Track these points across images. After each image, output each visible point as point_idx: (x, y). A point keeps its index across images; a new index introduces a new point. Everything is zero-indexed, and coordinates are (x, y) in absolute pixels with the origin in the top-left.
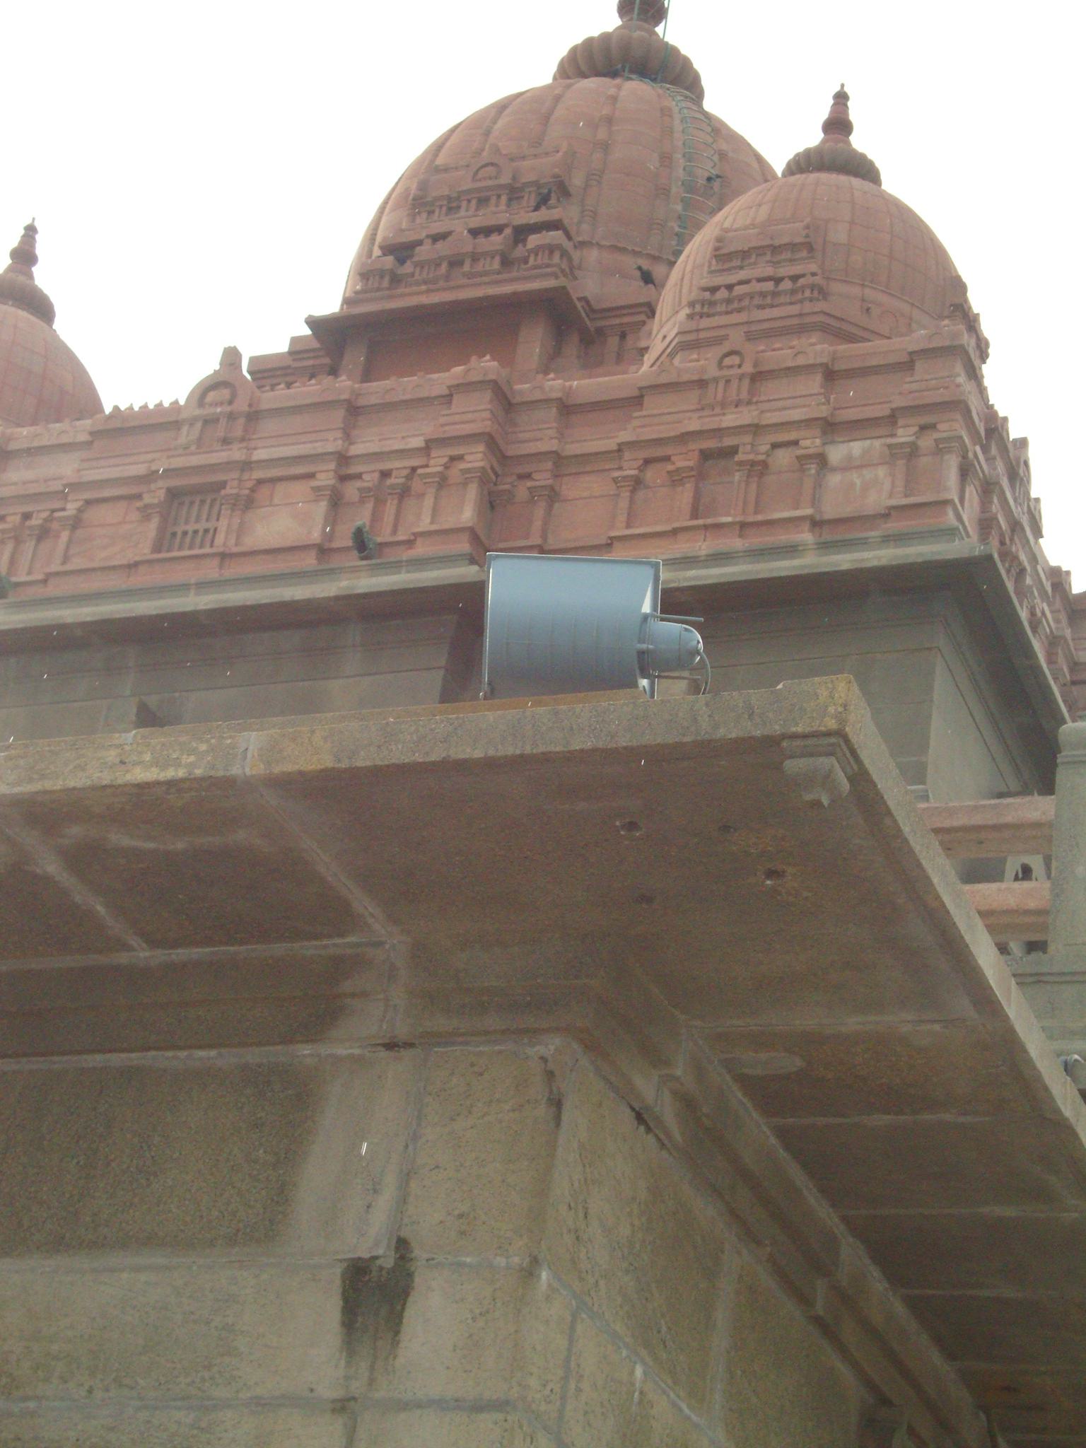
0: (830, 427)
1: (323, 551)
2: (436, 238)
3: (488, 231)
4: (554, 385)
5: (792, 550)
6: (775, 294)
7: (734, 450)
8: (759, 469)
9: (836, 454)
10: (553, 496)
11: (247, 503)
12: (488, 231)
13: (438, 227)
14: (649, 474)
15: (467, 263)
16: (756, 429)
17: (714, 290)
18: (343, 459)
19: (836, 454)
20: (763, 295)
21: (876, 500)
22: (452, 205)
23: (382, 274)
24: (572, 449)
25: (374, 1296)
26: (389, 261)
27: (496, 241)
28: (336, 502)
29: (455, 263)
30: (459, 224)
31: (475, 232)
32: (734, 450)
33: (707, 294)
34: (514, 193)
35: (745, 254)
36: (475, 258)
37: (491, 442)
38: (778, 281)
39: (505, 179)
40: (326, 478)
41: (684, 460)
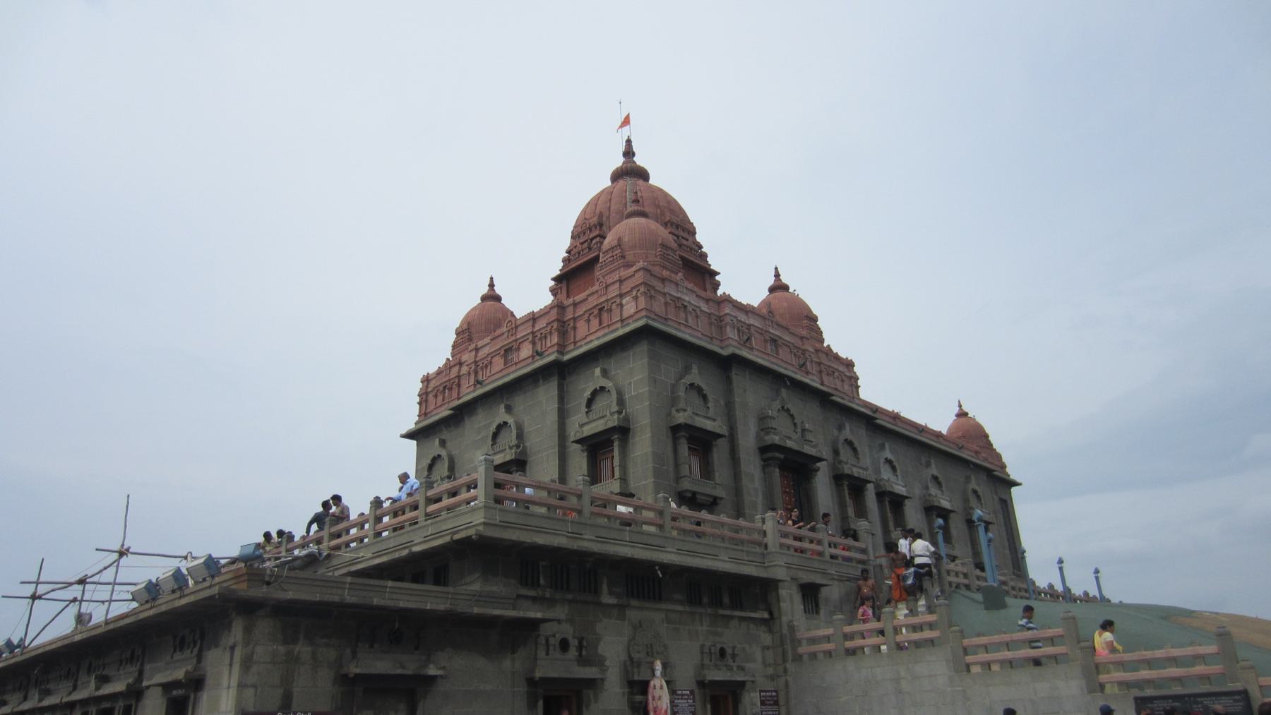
0: (621, 296)
1: (533, 357)
4: (571, 300)
5: (616, 330)
8: (610, 310)
9: (624, 302)
10: (575, 328)
11: (518, 349)
18: (533, 333)
19: (624, 302)
21: (633, 311)
25: (233, 648)
28: (534, 343)
37: (558, 320)
40: (530, 337)
41: (596, 312)
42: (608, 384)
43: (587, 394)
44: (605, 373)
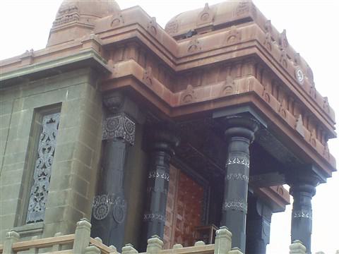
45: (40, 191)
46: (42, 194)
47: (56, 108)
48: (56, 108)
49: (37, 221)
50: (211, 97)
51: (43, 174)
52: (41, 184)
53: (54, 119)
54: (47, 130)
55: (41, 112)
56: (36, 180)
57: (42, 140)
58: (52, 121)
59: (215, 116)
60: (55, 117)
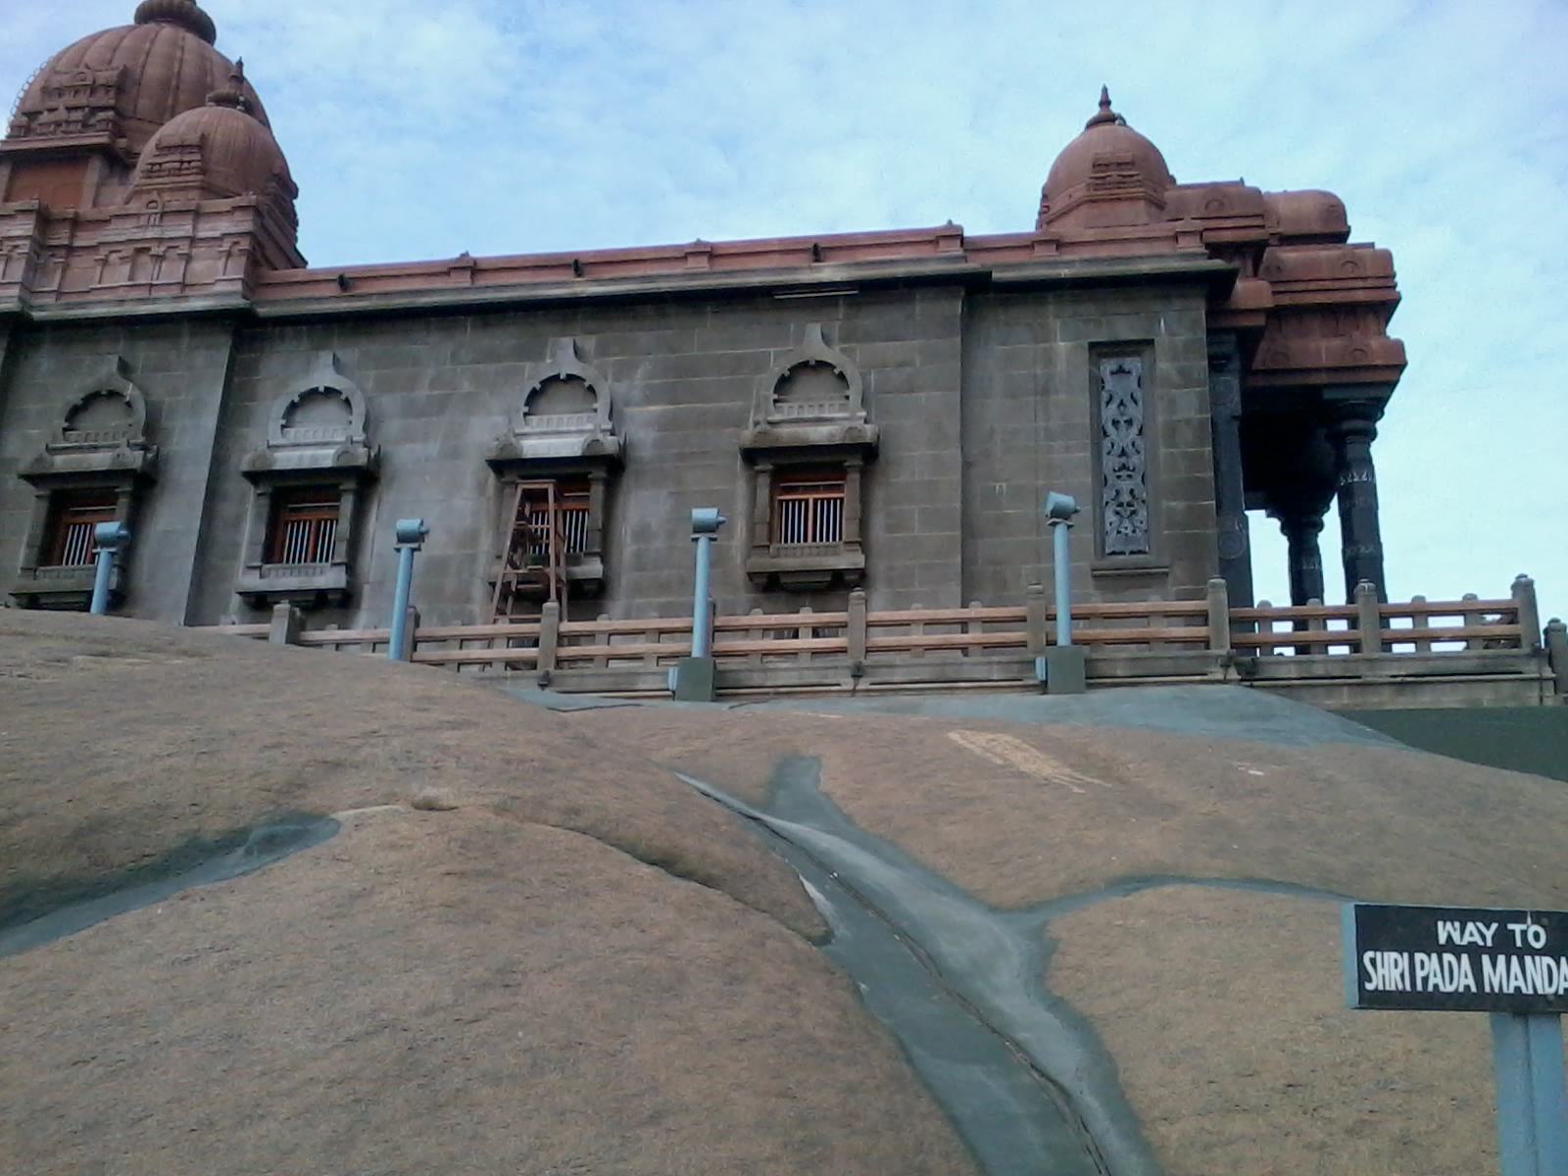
2: (52, 110)
3: (76, 108)
6: (180, 169)
7: (149, 249)
12: (76, 108)
13: (51, 104)
14: (113, 257)
15: (64, 125)
16: (160, 240)
17: (153, 165)
20: (174, 169)
22: (60, 92)
23: (20, 127)
24: (78, 243)
26: (25, 119)
27: (78, 115)
29: (58, 124)
30: (59, 104)
31: (69, 109)
32: (149, 249)
33: (150, 167)
34: (93, 89)
35: (169, 148)
36: (68, 122)
38: (182, 162)
39: (89, 82)
41: (128, 251)
42: (130, 391)
43: (75, 397)
44: (125, 368)
45: (1126, 498)
46: (1129, 505)
47: (1141, 346)
48: (1141, 346)
49: (1132, 553)
50: (1324, 362)
51: (1124, 467)
52: (1125, 485)
53: (1126, 367)
54: (1110, 384)
55: (1099, 350)
56: (1111, 479)
57: (1108, 403)
58: (1121, 371)
59: (1328, 395)
60: (1133, 364)
